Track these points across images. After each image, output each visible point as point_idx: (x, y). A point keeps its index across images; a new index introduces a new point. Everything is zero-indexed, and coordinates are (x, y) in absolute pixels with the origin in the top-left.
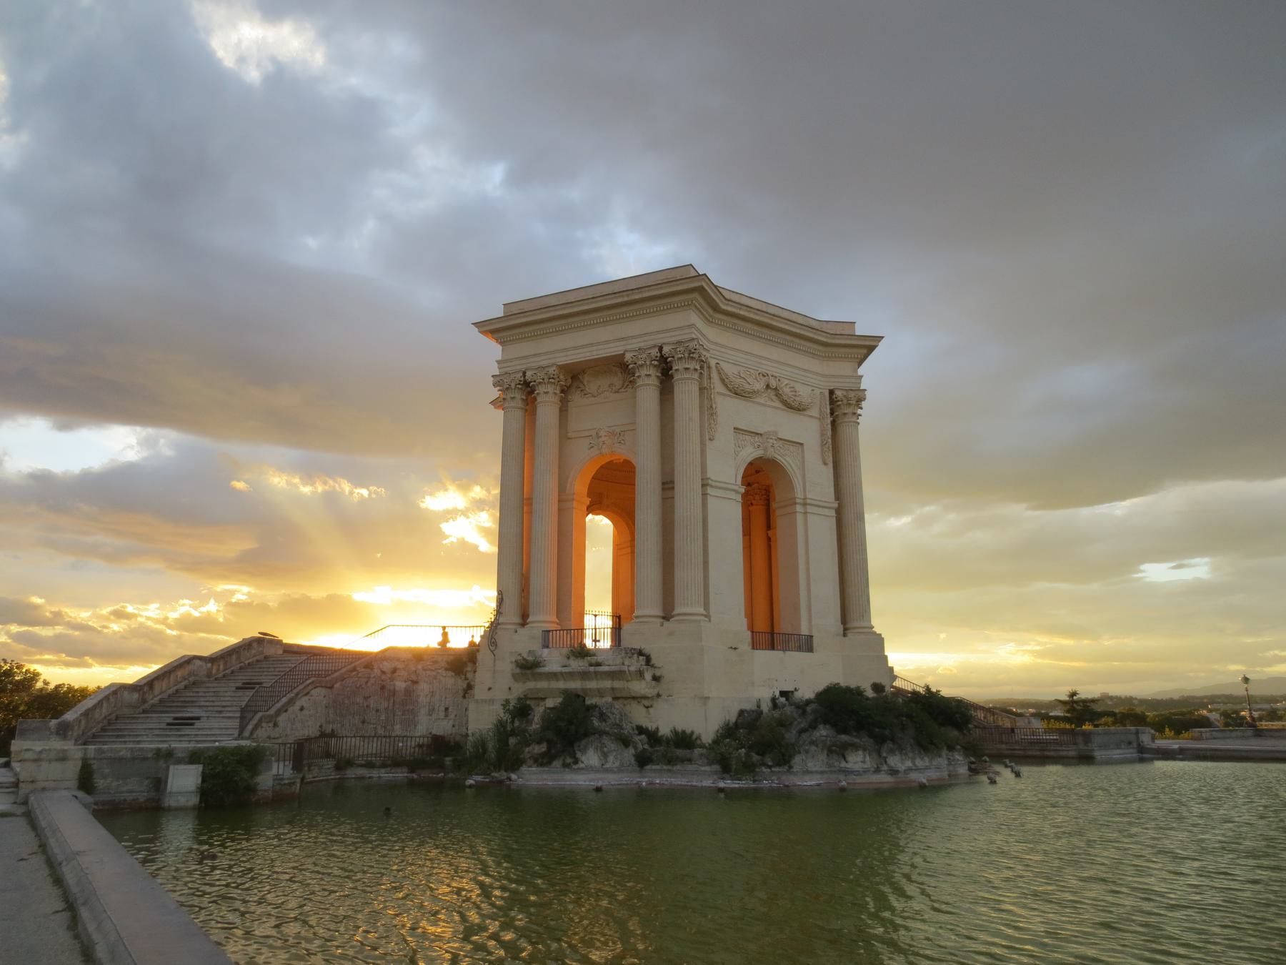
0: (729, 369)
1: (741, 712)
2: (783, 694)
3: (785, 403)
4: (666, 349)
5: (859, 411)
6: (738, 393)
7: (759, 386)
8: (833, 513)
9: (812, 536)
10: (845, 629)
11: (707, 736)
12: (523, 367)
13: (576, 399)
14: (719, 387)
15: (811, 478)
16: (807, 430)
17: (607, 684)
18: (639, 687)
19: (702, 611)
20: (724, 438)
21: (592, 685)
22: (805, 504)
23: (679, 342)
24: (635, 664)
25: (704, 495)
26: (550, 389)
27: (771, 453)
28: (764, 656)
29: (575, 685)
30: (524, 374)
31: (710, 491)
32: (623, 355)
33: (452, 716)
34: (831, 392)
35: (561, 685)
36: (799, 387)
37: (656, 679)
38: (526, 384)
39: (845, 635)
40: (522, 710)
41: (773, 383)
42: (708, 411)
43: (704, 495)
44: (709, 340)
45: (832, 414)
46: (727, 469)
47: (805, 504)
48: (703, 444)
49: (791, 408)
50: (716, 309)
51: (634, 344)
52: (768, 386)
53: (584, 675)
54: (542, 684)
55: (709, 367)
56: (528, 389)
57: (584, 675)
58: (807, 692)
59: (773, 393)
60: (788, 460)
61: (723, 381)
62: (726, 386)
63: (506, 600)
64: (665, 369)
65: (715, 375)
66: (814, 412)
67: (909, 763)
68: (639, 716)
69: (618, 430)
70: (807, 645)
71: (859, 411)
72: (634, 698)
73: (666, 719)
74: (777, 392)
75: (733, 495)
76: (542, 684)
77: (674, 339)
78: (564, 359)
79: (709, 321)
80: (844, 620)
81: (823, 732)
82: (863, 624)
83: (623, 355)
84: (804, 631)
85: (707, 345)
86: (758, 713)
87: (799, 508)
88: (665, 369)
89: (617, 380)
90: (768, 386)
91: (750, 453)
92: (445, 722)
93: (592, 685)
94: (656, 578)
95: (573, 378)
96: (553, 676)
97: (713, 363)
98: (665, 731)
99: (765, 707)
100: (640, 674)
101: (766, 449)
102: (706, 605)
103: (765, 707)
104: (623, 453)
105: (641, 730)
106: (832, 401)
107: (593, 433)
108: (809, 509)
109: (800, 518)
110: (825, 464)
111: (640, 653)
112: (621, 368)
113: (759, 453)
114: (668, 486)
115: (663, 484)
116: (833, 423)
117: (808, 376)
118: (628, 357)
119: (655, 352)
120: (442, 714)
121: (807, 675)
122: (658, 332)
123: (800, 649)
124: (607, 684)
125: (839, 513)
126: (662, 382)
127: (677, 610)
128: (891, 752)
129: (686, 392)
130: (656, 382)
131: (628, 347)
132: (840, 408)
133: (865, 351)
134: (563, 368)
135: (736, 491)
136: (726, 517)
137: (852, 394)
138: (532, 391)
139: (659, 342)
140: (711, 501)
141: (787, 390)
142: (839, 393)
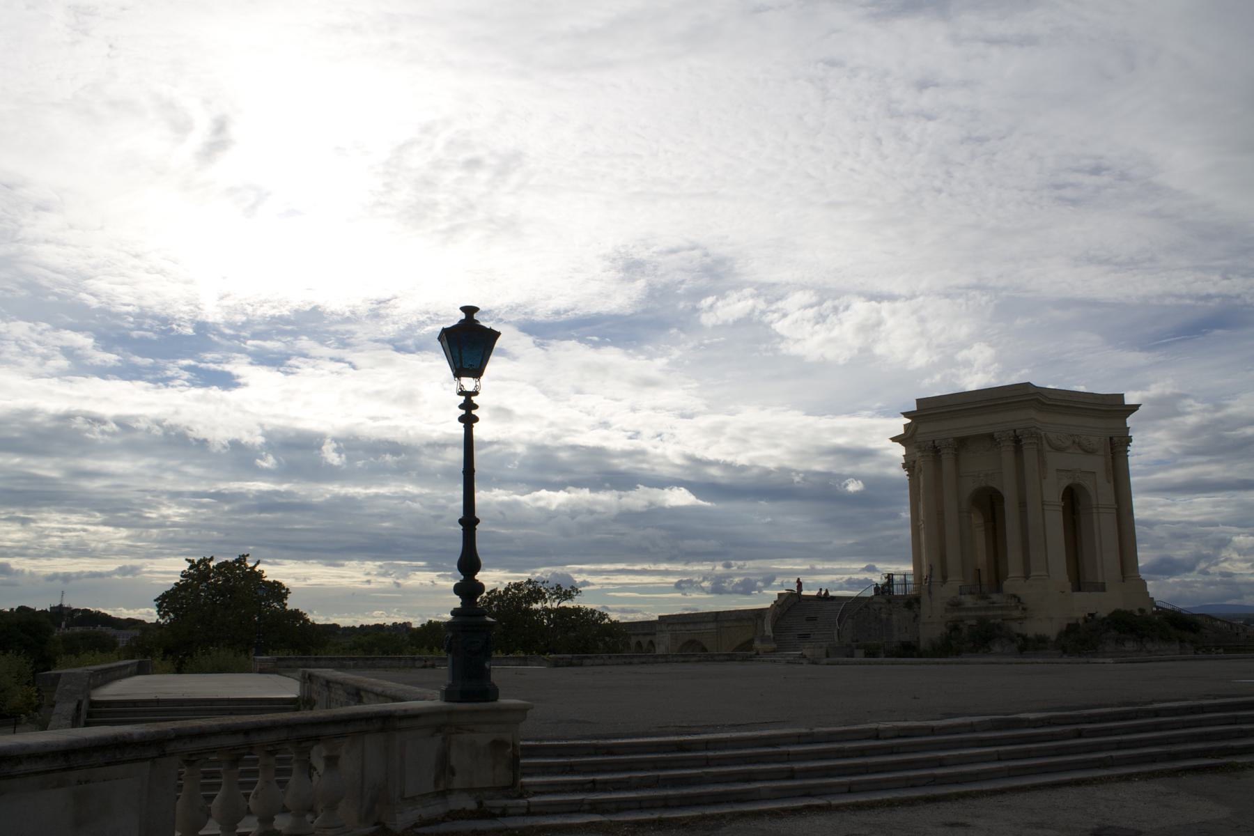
6: (1059, 449)
9: (1102, 525)
11: (1053, 638)
15: (1101, 493)
16: (1097, 464)
17: (1000, 612)
18: (1016, 614)
21: (991, 613)
29: (983, 613)
34: (1111, 438)
37: (1024, 609)
40: (955, 628)
46: (1054, 495)
50: (1043, 404)
54: (963, 614)
56: (936, 450)
58: (1103, 613)
64: (1017, 441)
68: (1016, 627)
70: (1102, 588)
73: (1032, 629)
74: (1080, 445)
76: (963, 614)
80: (1123, 573)
84: (1100, 581)
86: (1077, 625)
88: (1017, 441)
91: (1066, 482)
93: (991, 613)
95: (962, 443)
96: (969, 609)
98: (1031, 634)
99: (1081, 622)
103: (1081, 622)
105: (1019, 635)
111: (1015, 596)
114: (1023, 504)
116: (1113, 458)
118: (996, 435)
121: (1103, 604)
123: (1097, 590)
124: (1000, 612)
129: (1030, 455)
132: (1118, 445)
134: (955, 439)
136: (1055, 520)
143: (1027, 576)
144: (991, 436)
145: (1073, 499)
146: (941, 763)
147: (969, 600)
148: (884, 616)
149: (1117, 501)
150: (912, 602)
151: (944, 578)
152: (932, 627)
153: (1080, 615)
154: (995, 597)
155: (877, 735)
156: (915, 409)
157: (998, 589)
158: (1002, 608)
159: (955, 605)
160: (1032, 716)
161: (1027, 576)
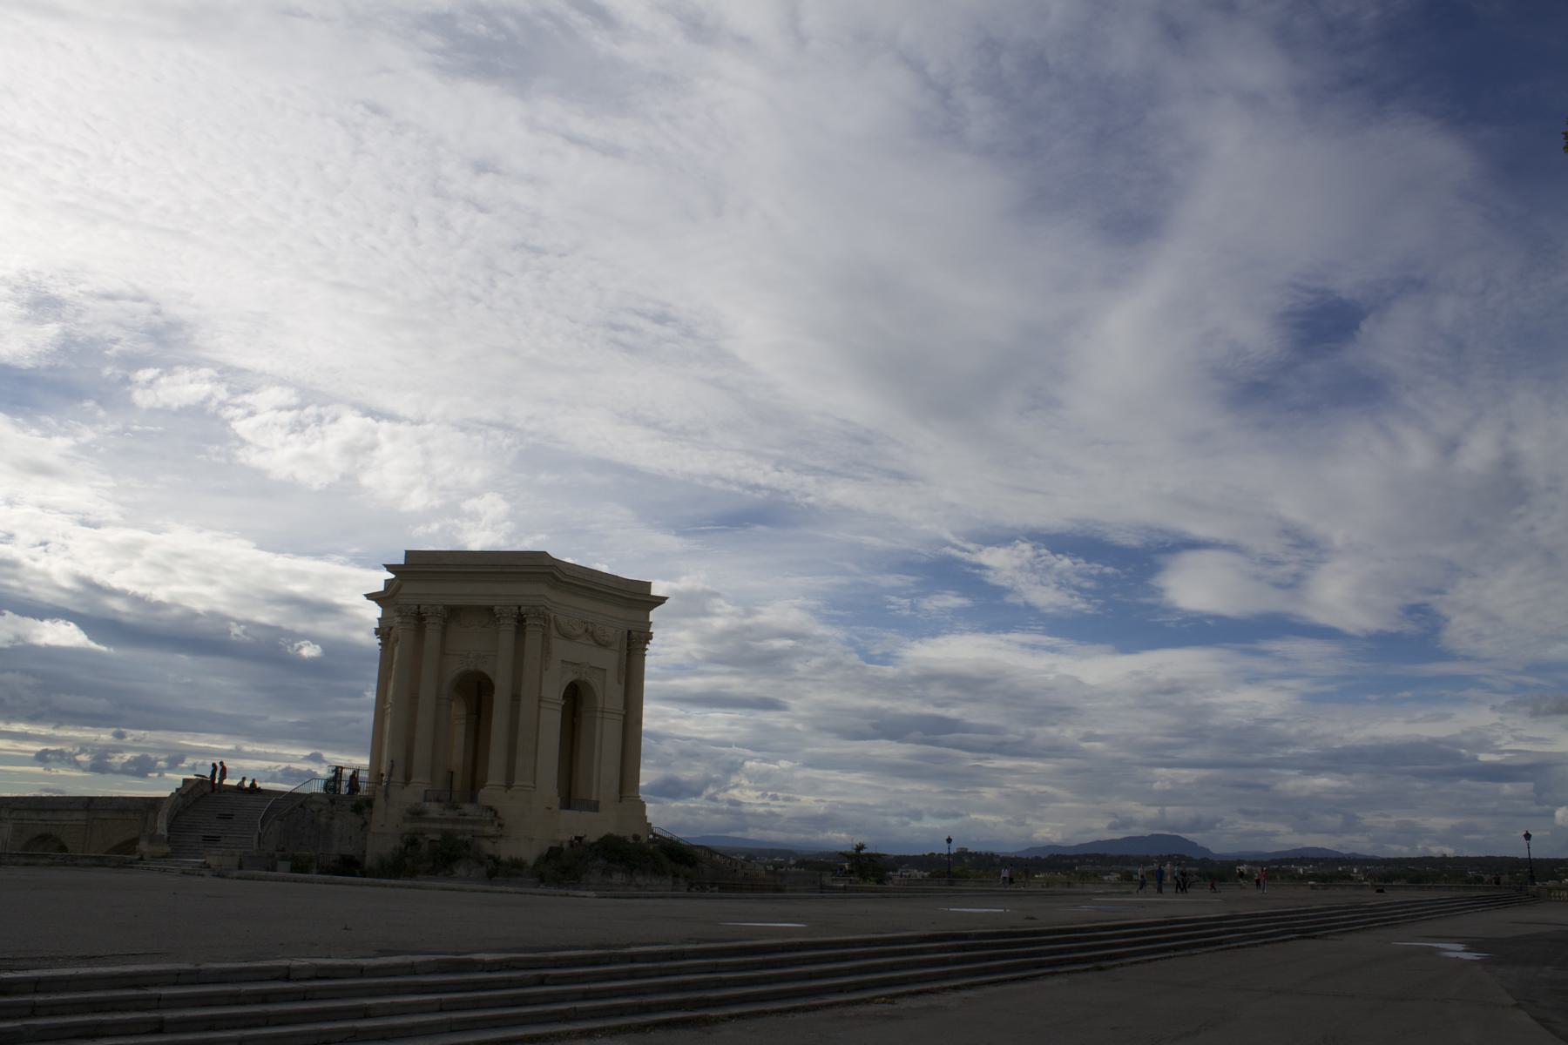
1: (551, 849)
4: (523, 609)
6: (567, 637)
9: (606, 732)
11: (531, 863)
14: (554, 633)
15: (609, 695)
16: (609, 660)
17: (470, 827)
18: (490, 830)
21: (459, 827)
24: (488, 816)
28: (566, 813)
35: (438, 826)
40: (413, 842)
46: (554, 691)
50: (558, 579)
53: (455, 821)
54: (424, 825)
56: (420, 618)
57: (455, 821)
58: (592, 838)
64: (521, 620)
68: (488, 847)
70: (594, 807)
73: (506, 850)
74: (592, 634)
76: (424, 825)
80: (621, 792)
81: (601, 862)
84: (594, 798)
88: (521, 620)
91: (570, 677)
93: (459, 827)
95: (453, 613)
96: (434, 820)
98: (504, 857)
99: (566, 846)
100: (492, 822)
103: (566, 846)
105: (490, 857)
109: (598, 721)
111: (491, 809)
112: (489, 613)
114: (516, 698)
118: (496, 609)
121: (593, 826)
124: (470, 827)
125: (625, 717)
129: (533, 639)
132: (637, 640)
134: (446, 607)
138: (423, 619)
143: (509, 786)
144: (490, 610)
145: (576, 698)
146: (366, 1013)
147: (434, 809)
148: (323, 820)
149: (626, 706)
150: (362, 806)
151: (408, 779)
152: (383, 839)
153: (565, 837)
154: (468, 808)
155: (287, 975)
156: (402, 562)
157: (473, 799)
158: (473, 822)
159: (417, 814)
160: (488, 957)
161: (509, 786)
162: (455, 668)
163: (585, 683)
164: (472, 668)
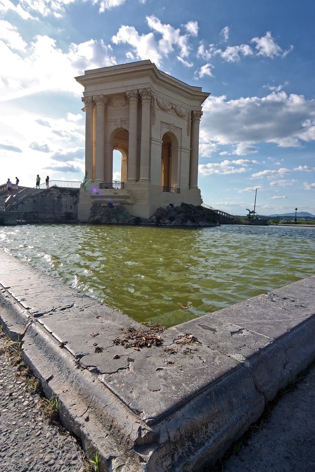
0: (160, 100)
2: (170, 205)
3: (177, 114)
4: (140, 91)
5: (200, 119)
6: (163, 109)
7: (169, 107)
8: (189, 152)
9: (182, 158)
10: (190, 188)
12: (91, 95)
13: (110, 108)
14: (157, 107)
16: (184, 124)
18: (129, 201)
19: (148, 179)
20: (157, 124)
22: (181, 148)
23: (145, 89)
25: (150, 143)
26: (101, 103)
27: (172, 131)
29: (109, 200)
30: (92, 97)
31: (152, 141)
32: (126, 92)
33: (73, 209)
34: (192, 112)
36: (182, 109)
38: (93, 101)
39: (189, 189)
41: (174, 107)
42: (152, 114)
43: (150, 143)
44: (154, 89)
45: (192, 120)
47: (181, 148)
48: (151, 126)
49: (179, 115)
50: (157, 77)
51: (130, 89)
52: (172, 108)
55: (154, 99)
59: (174, 110)
60: (177, 133)
61: (158, 104)
62: (159, 106)
63: (88, 174)
65: (155, 102)
66: (186, 118)
67: (204, 224)
69: (124, 119)
71: (200, 119)
72: (127, 204)
75: (159, 144)
77: (143, 87)
78: (105, 94)
79: (155, 82)
80: (190, 185)
82: (195, 186)
83: (126, 92)
85: (154, 91)
87: (179, 150)
89: (123, 102)
90: (172, 108)
91: (165, 130)
92: (71, 210)
94: (134, 168)
95: (108, 100)
97: (155, 97)
101: (170, 129)
102: (149, 178)
104: (124, 127)
106: (192, 115)
107: (116, 120)
108: (182, 149)
110: (188, 136)
112: (125, 97)
113: (168, 130)
115: (138, 139)
116: (192, 122)
117: (185, 105)
118: (127, 93)
119: (136, 92)
120: (70, 208)
122: (137, 85)
126: (138, 103)
127: (141, 178)
128: (200, 220)
130: (136, 103)
131: (127, 90)
132: (195, 116)
133: (204, 98)
135: (160, 143)
136: (157, 150)
137: (199, 113)
139: (138, 88)
140: (152, 145)
141: (178, 110)
142: (194, 112)
145: (168, 145)
149: (191, 146)
150: (73, 193)
152: (84, 206)
153: (165, 205)
162: (112, 128)
163: (173, 135)
164: (119, 126)
